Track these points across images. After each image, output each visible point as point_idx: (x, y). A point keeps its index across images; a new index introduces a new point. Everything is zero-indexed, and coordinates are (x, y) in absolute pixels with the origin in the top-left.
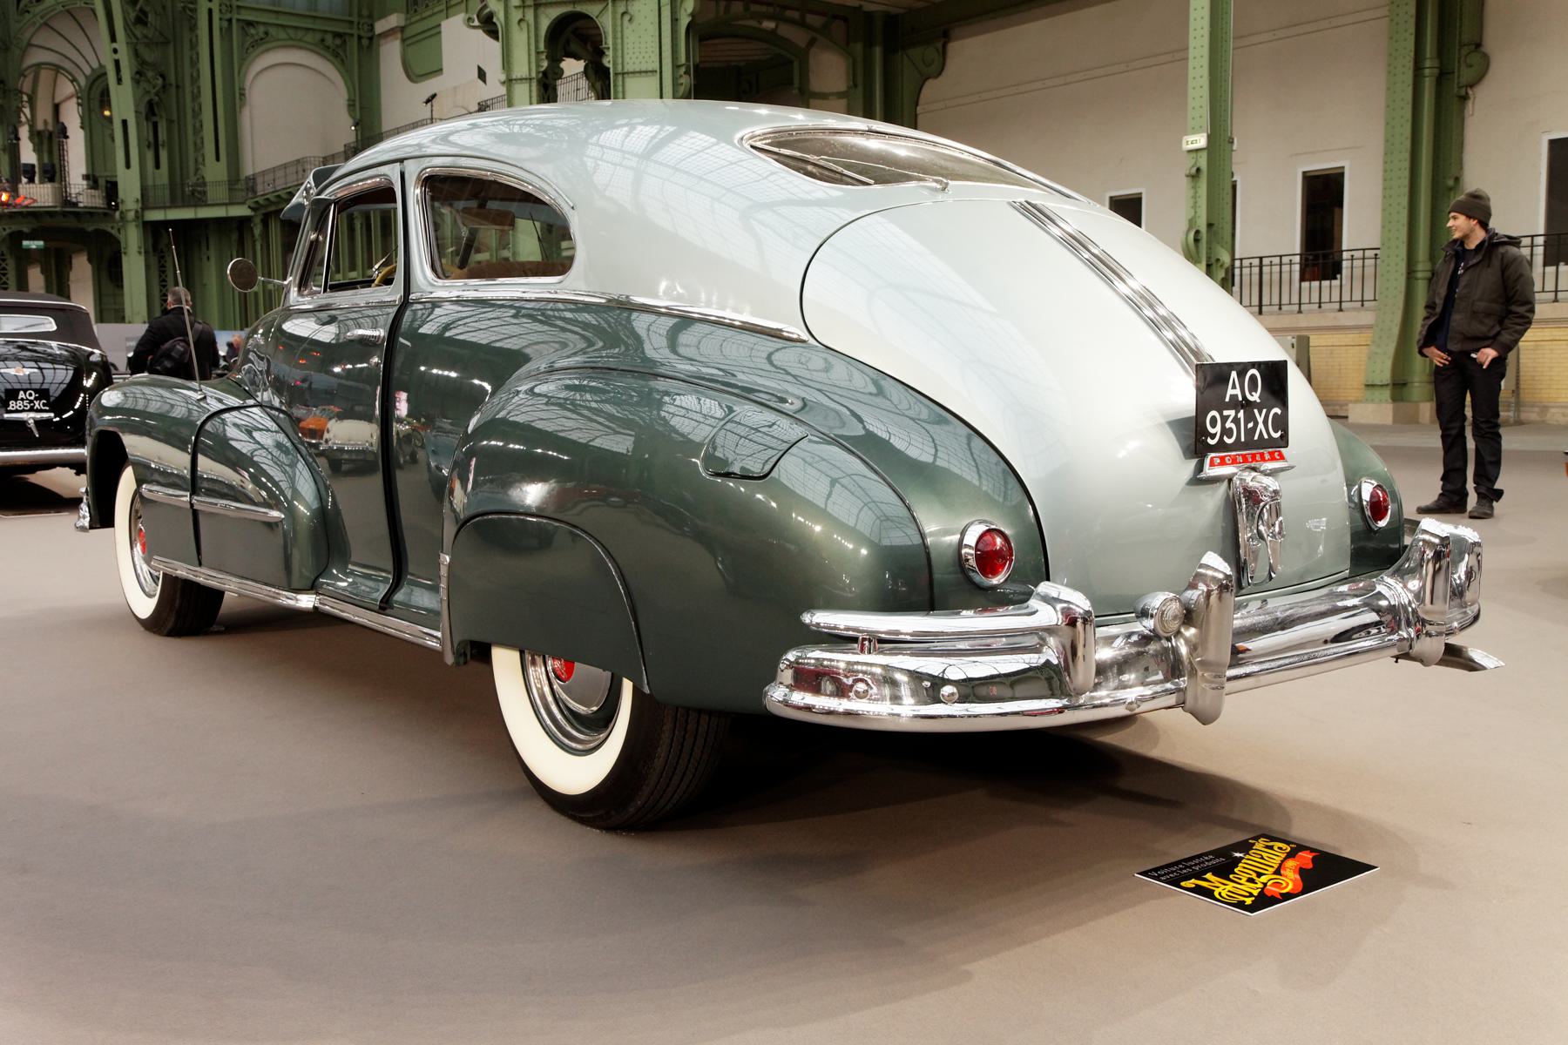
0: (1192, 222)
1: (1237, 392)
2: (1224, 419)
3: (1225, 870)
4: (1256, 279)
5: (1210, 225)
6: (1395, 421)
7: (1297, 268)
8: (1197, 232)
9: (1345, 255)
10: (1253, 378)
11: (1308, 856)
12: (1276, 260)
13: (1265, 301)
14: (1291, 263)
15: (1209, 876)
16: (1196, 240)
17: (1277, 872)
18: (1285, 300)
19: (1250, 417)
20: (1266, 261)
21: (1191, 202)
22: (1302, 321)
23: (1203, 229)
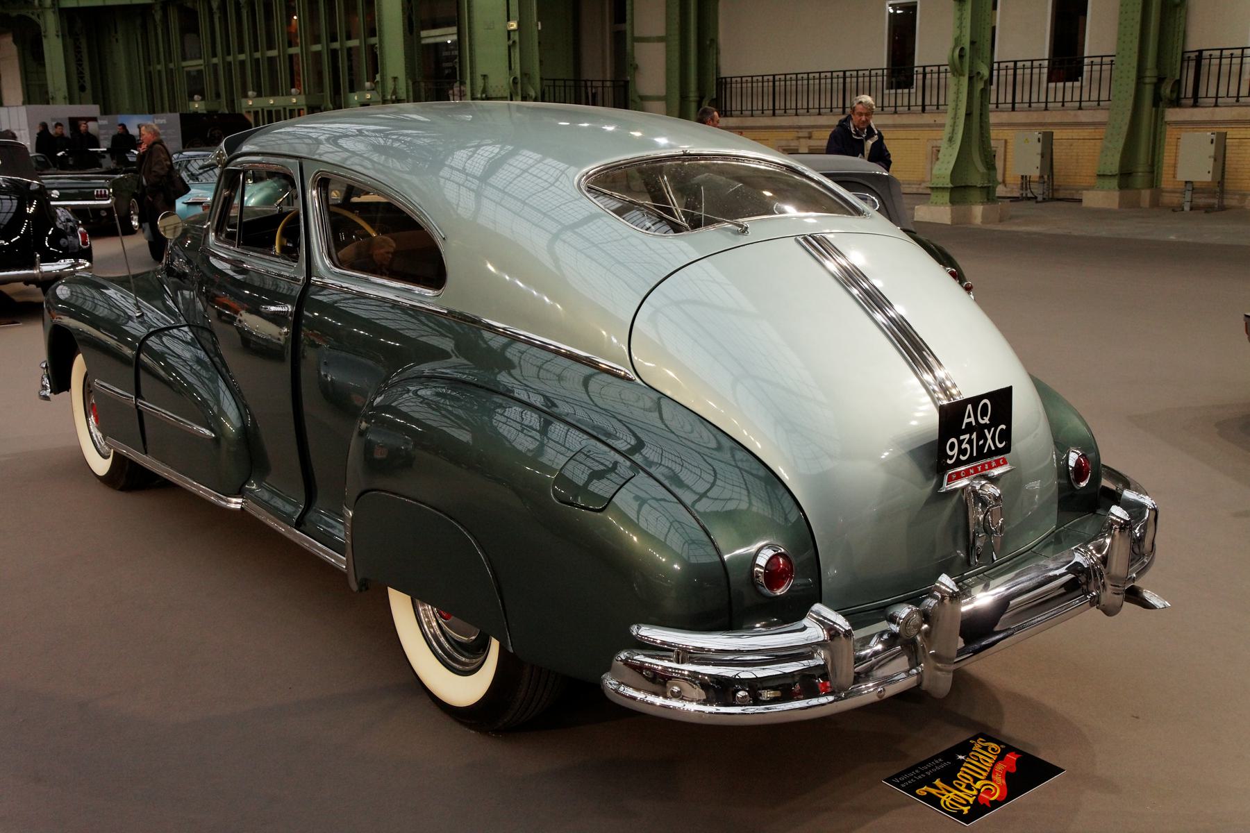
0: (957, 40)
1: (972, 419)
2: (960, 443)
3: (949, 777)
4: (1010, 78)
5: (973, 43)
6: (1120, 205)
7: (1045, 70)
8: (962, 49)
9: (1086, 61)
10: (985, 405)
11: (1012, 757)
12: (1028, 64)
13: (1018, 99)
14: (1040, 67)
15: (937, 782)
16: (961, 56)
17: (989, 778)
18: (1034, 99)
19: (982, 436)
20: (1020, 65)
21: (958, 23)
22: (1049, 117)
23: (967, 46)
